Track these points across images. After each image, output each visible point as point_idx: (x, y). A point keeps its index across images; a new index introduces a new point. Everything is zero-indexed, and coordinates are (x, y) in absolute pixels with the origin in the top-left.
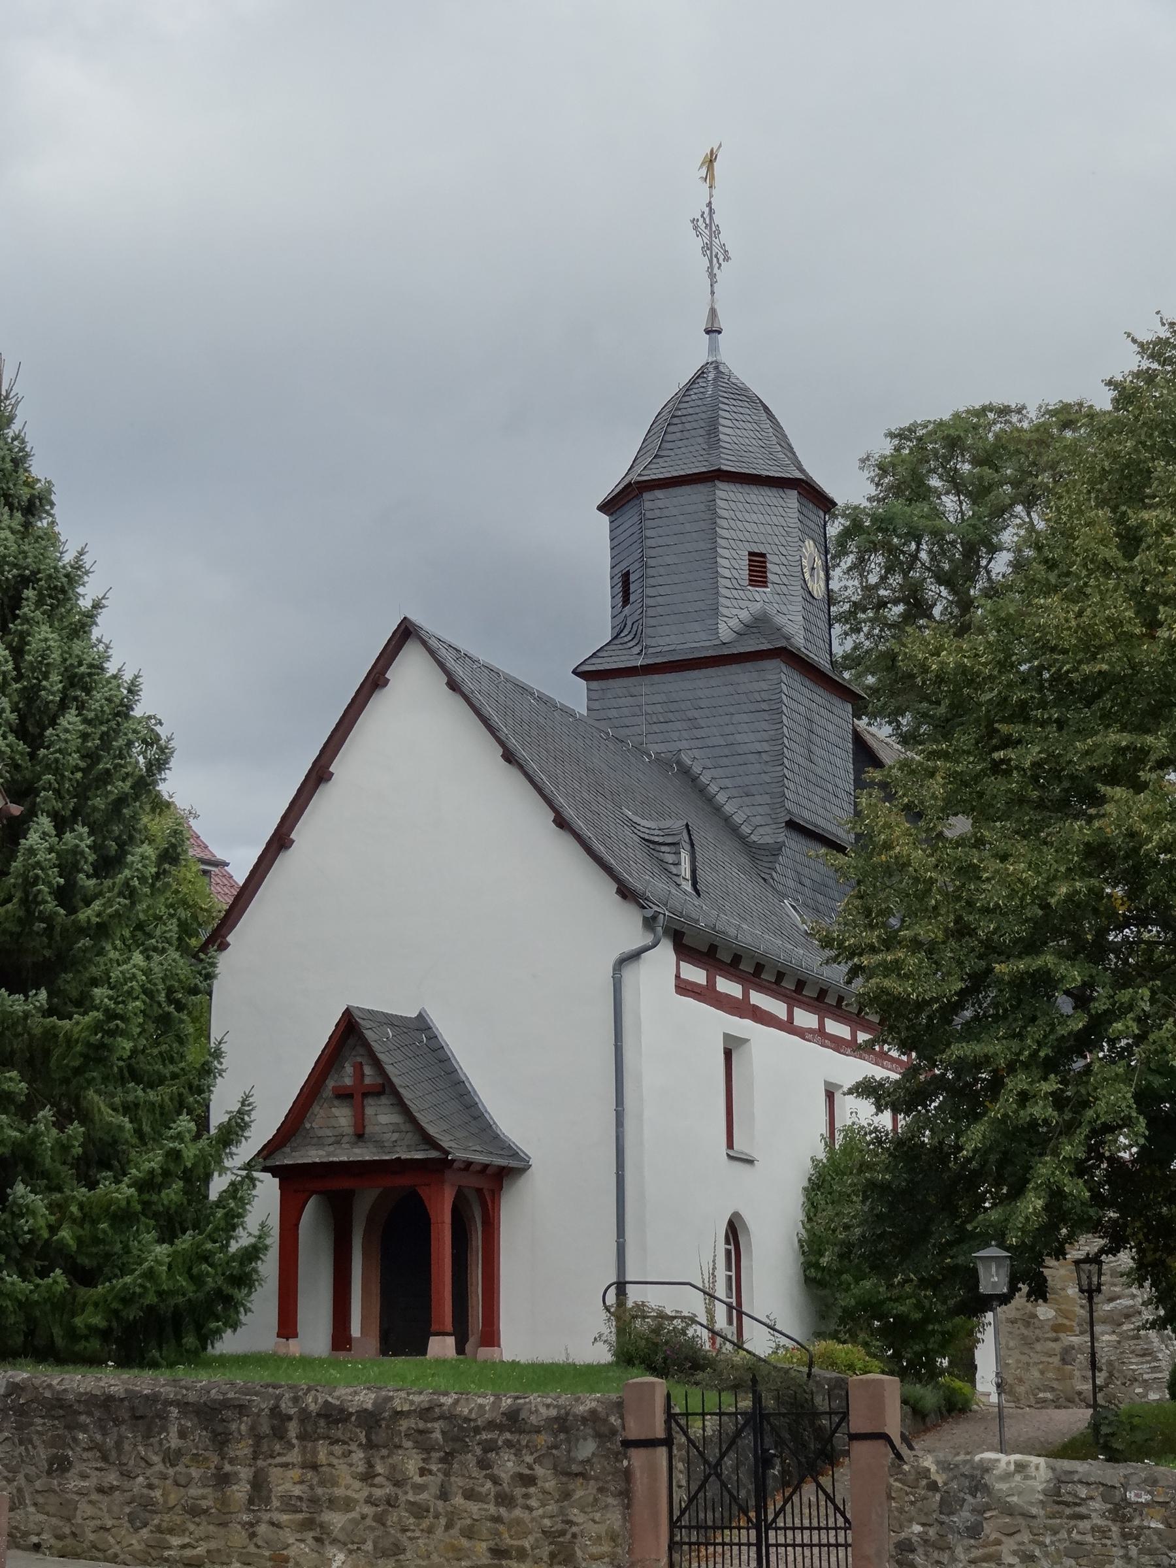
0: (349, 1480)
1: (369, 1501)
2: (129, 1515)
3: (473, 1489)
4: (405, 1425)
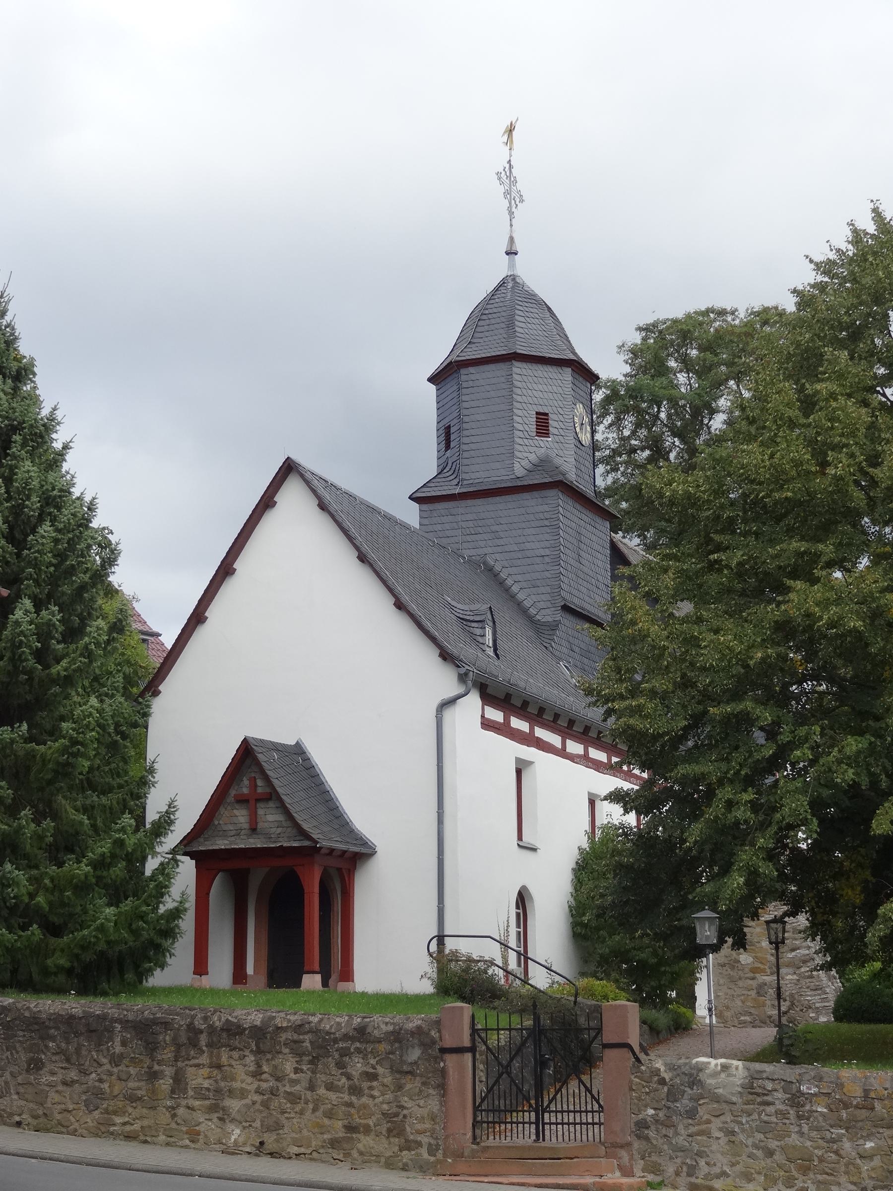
0: (244, 1076)
1: (258, 1091)
2: (85, 1101)
3: (332, 1083)
4: (284, 1036)
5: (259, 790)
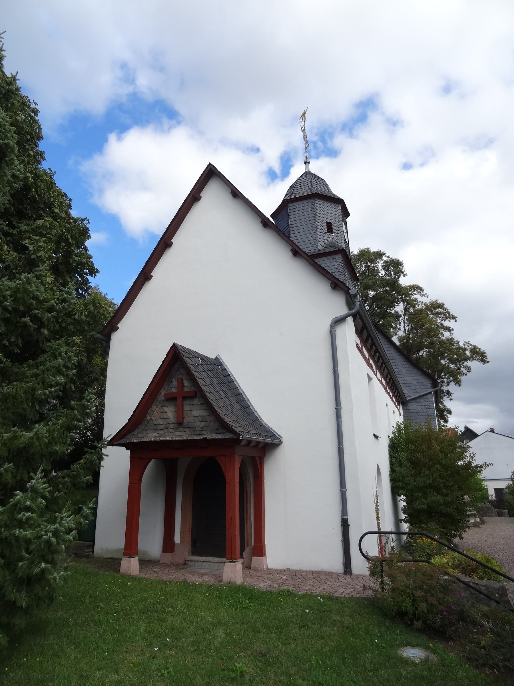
5: (186, 389)
